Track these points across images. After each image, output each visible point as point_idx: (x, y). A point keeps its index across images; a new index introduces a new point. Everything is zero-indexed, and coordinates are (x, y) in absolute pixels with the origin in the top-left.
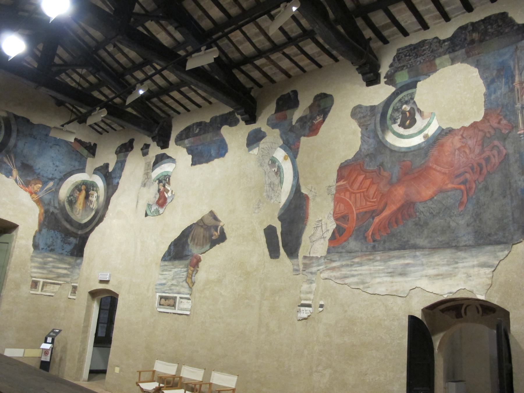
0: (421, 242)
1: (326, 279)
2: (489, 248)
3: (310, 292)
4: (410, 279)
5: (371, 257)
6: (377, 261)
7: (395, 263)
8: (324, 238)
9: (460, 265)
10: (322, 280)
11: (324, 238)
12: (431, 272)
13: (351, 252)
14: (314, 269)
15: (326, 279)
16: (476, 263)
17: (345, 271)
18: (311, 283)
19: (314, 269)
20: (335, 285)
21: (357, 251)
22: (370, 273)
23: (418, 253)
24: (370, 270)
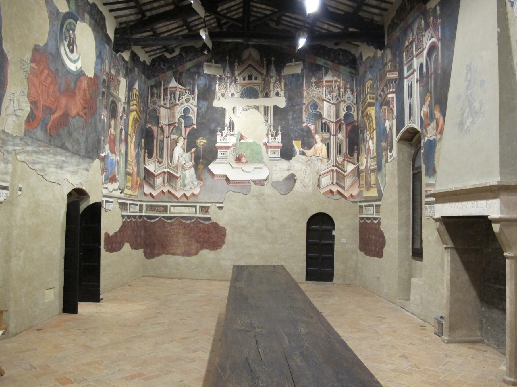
0: (69, 147)
1: (23, 162)
2: (88, 160)
3: (6, 173)
4: (63, 172)
5: (48, 149)
6: (51, 153)
7: (60, 158)
8: (15, 115)
9: (80, 167)
10: (20, 163)
11: (15, 115)
12: (71, 169)
13: (38, 140)
14: (10, 148)
15: (23, 162)
16: (84, 167)
17: (34, 157)
18: (7, 163)
19: (10, 148)
20: (28, 169)
21: (41, 141)
22: (48, 163)
23: (68, 154)
24: (47, 160)
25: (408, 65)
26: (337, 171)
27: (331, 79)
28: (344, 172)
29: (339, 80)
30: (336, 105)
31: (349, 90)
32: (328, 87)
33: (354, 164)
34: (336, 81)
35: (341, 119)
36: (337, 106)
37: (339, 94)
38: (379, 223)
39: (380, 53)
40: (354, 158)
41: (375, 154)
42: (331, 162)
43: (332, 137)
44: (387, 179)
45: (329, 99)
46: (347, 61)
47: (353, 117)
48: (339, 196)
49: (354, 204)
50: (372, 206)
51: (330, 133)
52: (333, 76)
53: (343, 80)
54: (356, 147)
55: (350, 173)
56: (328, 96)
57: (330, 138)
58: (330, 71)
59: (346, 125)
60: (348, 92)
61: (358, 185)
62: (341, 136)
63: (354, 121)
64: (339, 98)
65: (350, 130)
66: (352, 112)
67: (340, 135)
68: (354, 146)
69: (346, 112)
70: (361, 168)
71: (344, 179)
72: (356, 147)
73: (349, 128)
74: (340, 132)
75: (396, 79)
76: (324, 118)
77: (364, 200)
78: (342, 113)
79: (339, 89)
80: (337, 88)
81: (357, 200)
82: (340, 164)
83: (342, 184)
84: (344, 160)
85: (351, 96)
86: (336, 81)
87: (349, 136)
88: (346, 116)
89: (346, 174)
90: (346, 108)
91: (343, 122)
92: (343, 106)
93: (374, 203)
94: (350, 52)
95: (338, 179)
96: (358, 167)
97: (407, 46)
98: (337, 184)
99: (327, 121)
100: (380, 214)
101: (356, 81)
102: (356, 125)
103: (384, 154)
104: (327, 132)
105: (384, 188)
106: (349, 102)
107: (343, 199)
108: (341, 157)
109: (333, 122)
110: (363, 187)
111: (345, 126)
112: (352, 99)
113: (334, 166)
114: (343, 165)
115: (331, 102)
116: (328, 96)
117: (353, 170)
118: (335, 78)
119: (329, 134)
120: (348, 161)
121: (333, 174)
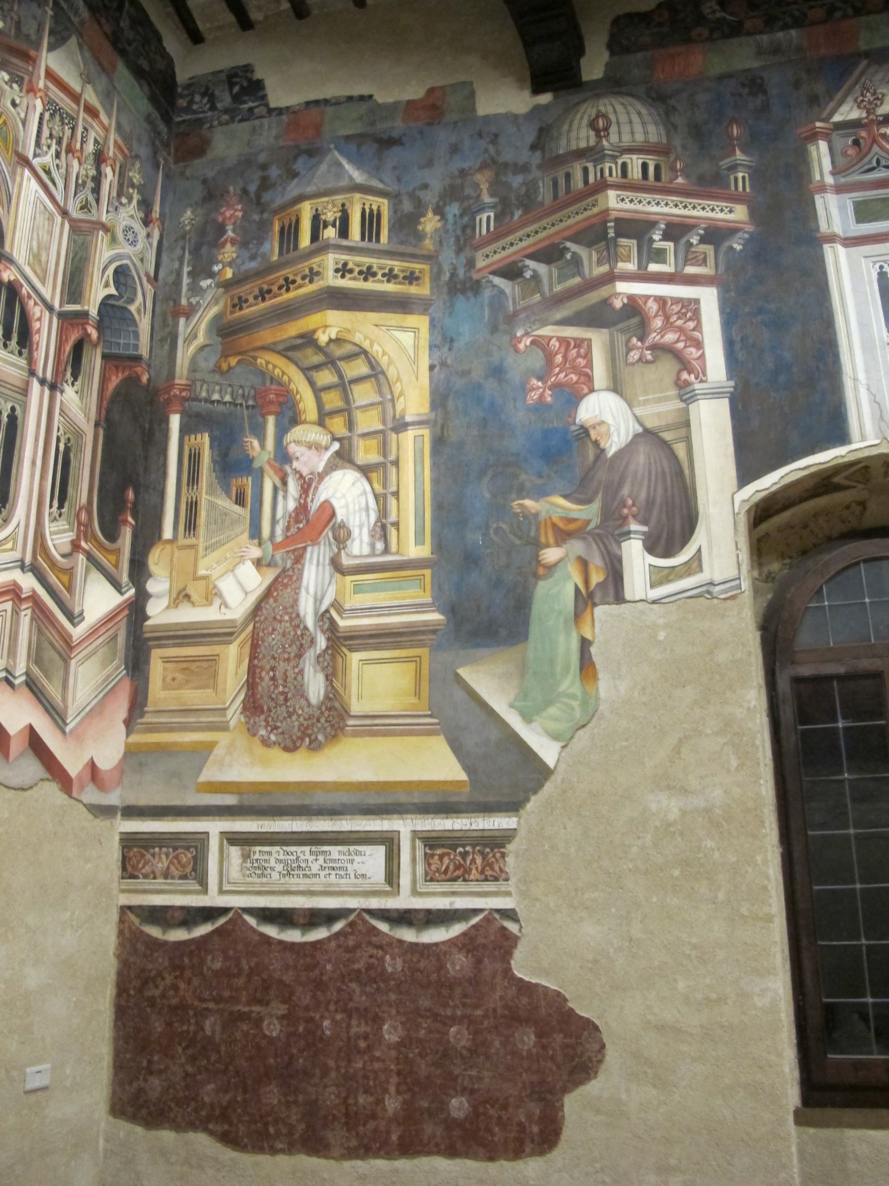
25: (859, 195)
26: (34, 598)
27: (75, 85)
28: (71, 617)
29: (103, 117)
30: (76, 228)
31: (136, 197)
32: (53, 110)
33: (117, 586)
34: (91, 111)
35: (85, 314)
36: (82, 234)
37: (97, 180)
38: (492, 940)
39: (506, 99)
40: (118, 552)
41: (416, 549)
42: (13, 537)
43: (36, 386)
44: (604, 686)
45: (48, 172)
46: (145, 65)
47: (136, 335)
48: (32, 769)
49: (101, 824)
50: (390, 841)
51: (31, 360)
52: (87, 79)
53: (119, 127)
54: (131, 495)
55: (94, 632)
56: (48, 159)
57: (25, 391)
58: (73, 41)
59: (104, 356)
60: (130, 199)
61: (123, 713)
62: (78, 404)
63: (138, 359)
64: (91, 198)
65: (117, 392)
66: (133, 308)
67: (70, 395)
68: (123, 490)
69: (112, 290)
70: (158, 612)
71: (66, 661)
72: (131, 495)
73: (115, 381)
74: (75, 376)
75: (715, 235)
76: (11, 261)
77: (230, 800)
78: (98, 290)
79: (99, 158)
80: (90, 147)
81: (113, 798)
82: (53, 564)
83: (53, 691)
84: (75, 546)
85: (142, 232)
86: (91, 111)
87: (107, 420)
88: (105, 303)
89: (77, 632)
90: (116, 272)
91: (94, 334)
92: (103, 253)
93: (404, 827)
94: (159, 39)
95: (37, 657)
96: (136, 610)
97: (856, 124)
98: (32, 685)
99: (25, 290)
100: (511, 886)
101: (167, 176)
102: (145, 379)
103: (551, 555)
104: (13, 343)
105: (565, 740)
106: (127, 249)
107: (52, 790)
108: (62, 524)
109: (50, 308)
110: (223, 727)
111: (98, 362)
112: (140, 246)
113: (22, 567)
114: (70, 572)
115: (59, 198)
116: (48, 159)
117: (111, 618)
118: (91, 96)
119: (23, 362)
120: (90, 557)
121: (16, 612)
